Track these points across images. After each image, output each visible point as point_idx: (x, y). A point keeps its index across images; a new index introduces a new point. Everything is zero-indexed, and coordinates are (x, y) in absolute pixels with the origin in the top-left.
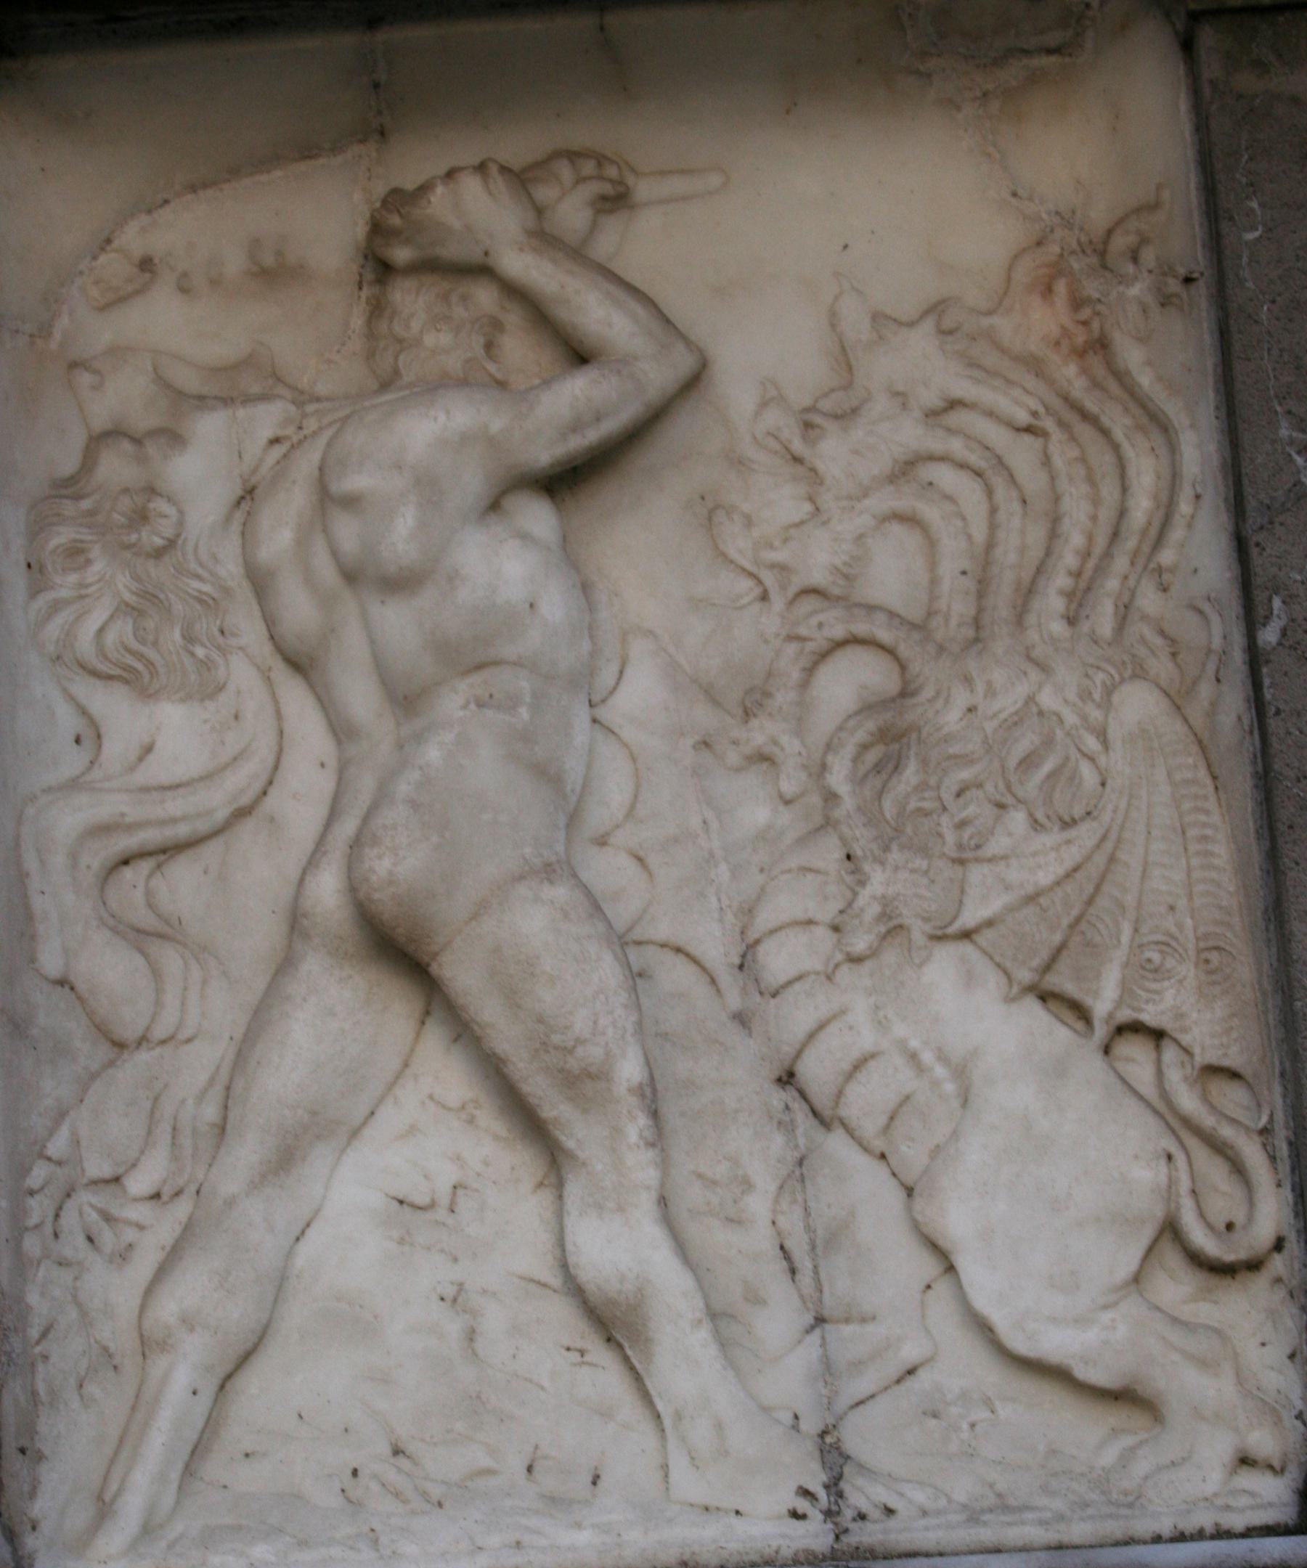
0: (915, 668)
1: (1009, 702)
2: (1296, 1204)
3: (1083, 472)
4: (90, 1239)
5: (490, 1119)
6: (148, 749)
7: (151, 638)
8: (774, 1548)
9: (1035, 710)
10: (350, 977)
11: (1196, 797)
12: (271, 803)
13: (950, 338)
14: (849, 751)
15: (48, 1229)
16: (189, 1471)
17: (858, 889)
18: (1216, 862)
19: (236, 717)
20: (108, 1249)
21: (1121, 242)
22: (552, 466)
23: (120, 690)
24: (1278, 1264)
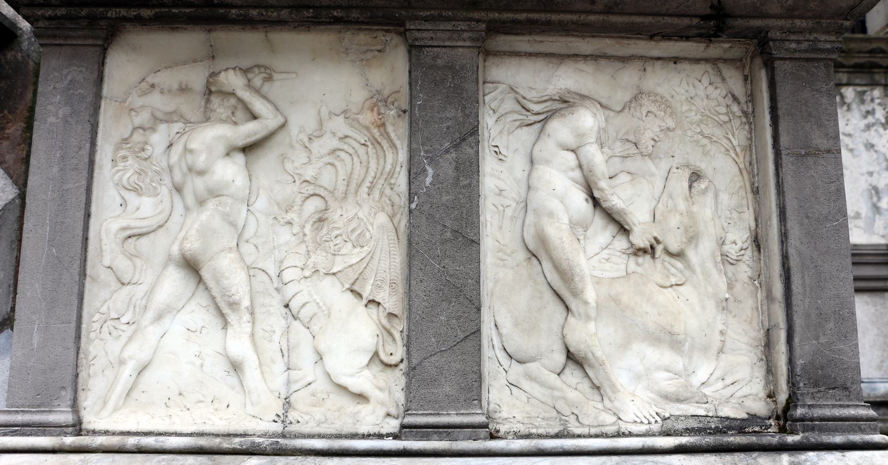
0: (329, 203)
1: (351, 214)
4: (110, 334)
5: (212, 309)
6: (138, 209)
7: (142, 180)
11: (394, 244)
14: (311, 223)
15: (98, 331)
16: (128, 394)
18: (397, 261)
21: (390, 100)
23: (133, 193)
24: (402, 366)
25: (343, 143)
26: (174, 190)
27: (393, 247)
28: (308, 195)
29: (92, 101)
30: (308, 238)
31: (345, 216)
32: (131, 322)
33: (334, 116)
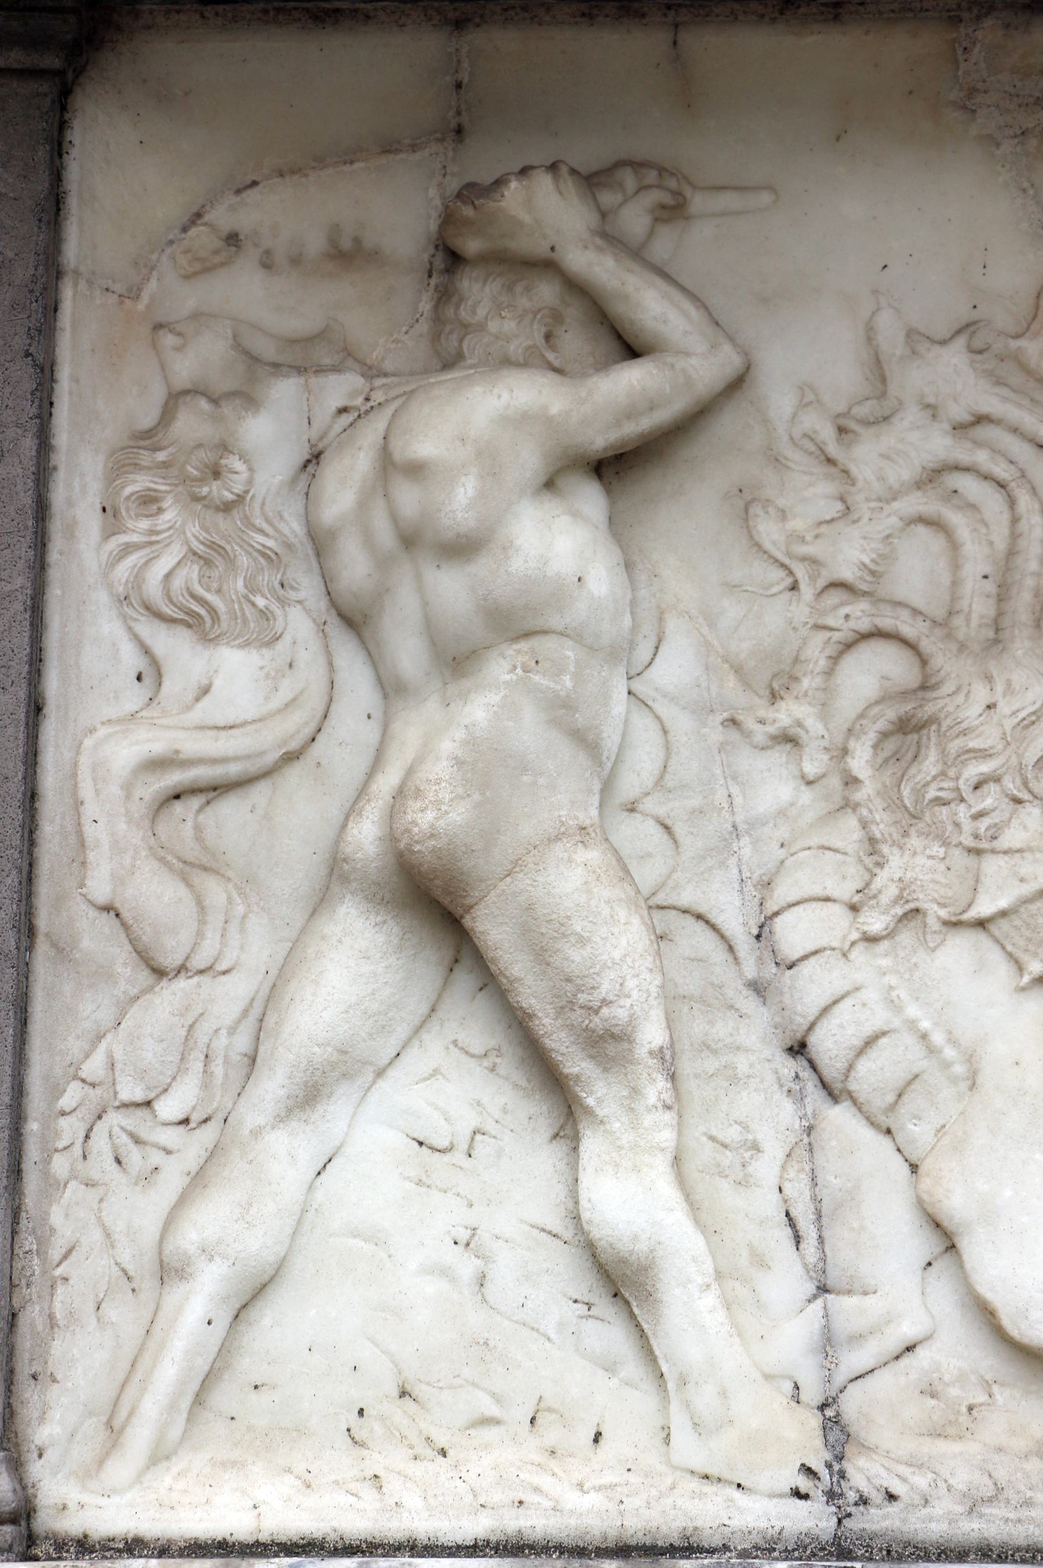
4: (118, 1161)
5: (508, 1065)
6: (205, 690)
7: (215, 585)
8: (777, 1529)
10: (385, 922)
12: (317, 750)
13: (979, 357)
14: (872, 736)
15: (77, 1150)
16: (199, 1400)
17: (877, 870)
19: (291, 666)
20: (134, 1171)
22: (605, 449)
25: (969, 445)
26: (333, 620)
28: (851, 636)
29: (34, 280)
30: (867, 791)
31: (1004, 708)
32: (195, 1118)
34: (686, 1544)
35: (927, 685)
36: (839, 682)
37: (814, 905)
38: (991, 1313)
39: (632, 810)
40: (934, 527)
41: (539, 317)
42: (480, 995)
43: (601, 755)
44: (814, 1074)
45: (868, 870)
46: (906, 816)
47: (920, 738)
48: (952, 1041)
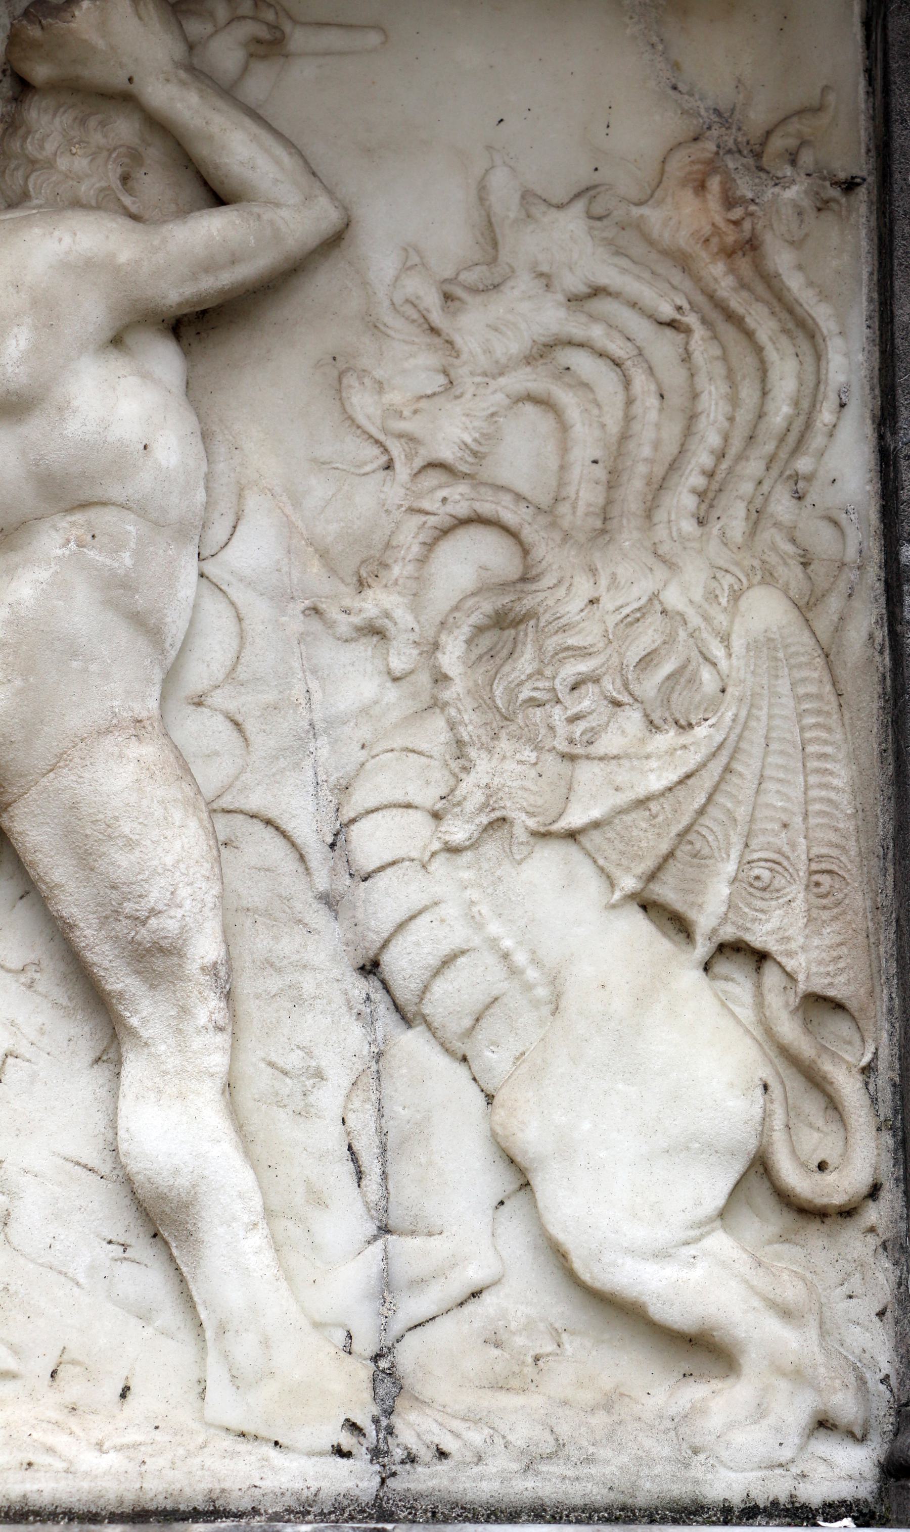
2: (896, 1151)
3: (723, 372)
9: (659, 608)
11: (819, 712)
13: (598, 224)
14: (465, 631)
17: (463, 776)
18: (836, 782)
21: (778, 143)
22: (180, 305)
24: (873, 1214)
25: (583, 319)
27: (817, 726)
28: (448, 522)
30: (456, 689)
31: (608, 603)
33: (543, 207)
34: (212, 1508)
35: (528, 576)
36: (433, 570)
37: (394, 811)
38: (563, 1256)
39: (199, 704)
40: (543, 407)
41: (114, 155)
42: (20, 904)
43: (164, 641)
44: (387, 995)
45: (455, 775)
46: (498, 717)
47: (517, 634)
48: (536, 961)
